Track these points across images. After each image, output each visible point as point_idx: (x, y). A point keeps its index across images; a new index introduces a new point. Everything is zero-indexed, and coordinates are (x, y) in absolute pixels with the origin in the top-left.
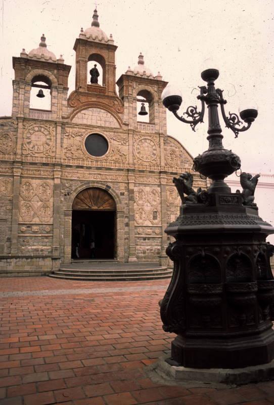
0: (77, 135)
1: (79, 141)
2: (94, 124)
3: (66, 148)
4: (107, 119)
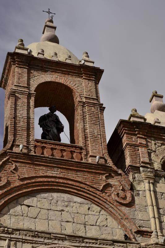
4: (91, 219)
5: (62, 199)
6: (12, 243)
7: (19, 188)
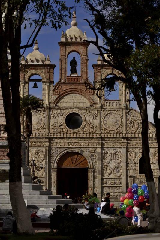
0: (59, 115)
1: (62, 119)
2: (71, 105)
3: (52, 125)
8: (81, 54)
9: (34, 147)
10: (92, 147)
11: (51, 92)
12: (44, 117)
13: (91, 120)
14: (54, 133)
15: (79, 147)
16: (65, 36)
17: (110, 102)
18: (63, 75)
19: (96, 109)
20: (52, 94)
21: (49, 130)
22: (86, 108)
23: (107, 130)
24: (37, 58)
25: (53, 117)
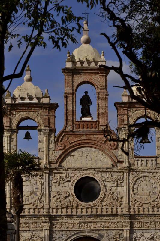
0: (64, 181)
1: (69, 187)
2: (84, 165)
3: (54, 197)
4: (99, 158)
5: (87, 150)
6: (68, 174)
7: (70, 148)
8: (96, 87)
9: (27, 230)
10: (116, 230)
11: (51, 146)
12: (42, 185)
13: (114, 188)
14: (57, 209)
15: (96, 230)
16: (72, 59)
17: (142, 159)
18: (70, 118)
19: (121, 171)
20: (53, 149)
21: (49, 204)
22: (106, 170)
23: (138, 203)
24: (29, 94)
25: (55, 184)
